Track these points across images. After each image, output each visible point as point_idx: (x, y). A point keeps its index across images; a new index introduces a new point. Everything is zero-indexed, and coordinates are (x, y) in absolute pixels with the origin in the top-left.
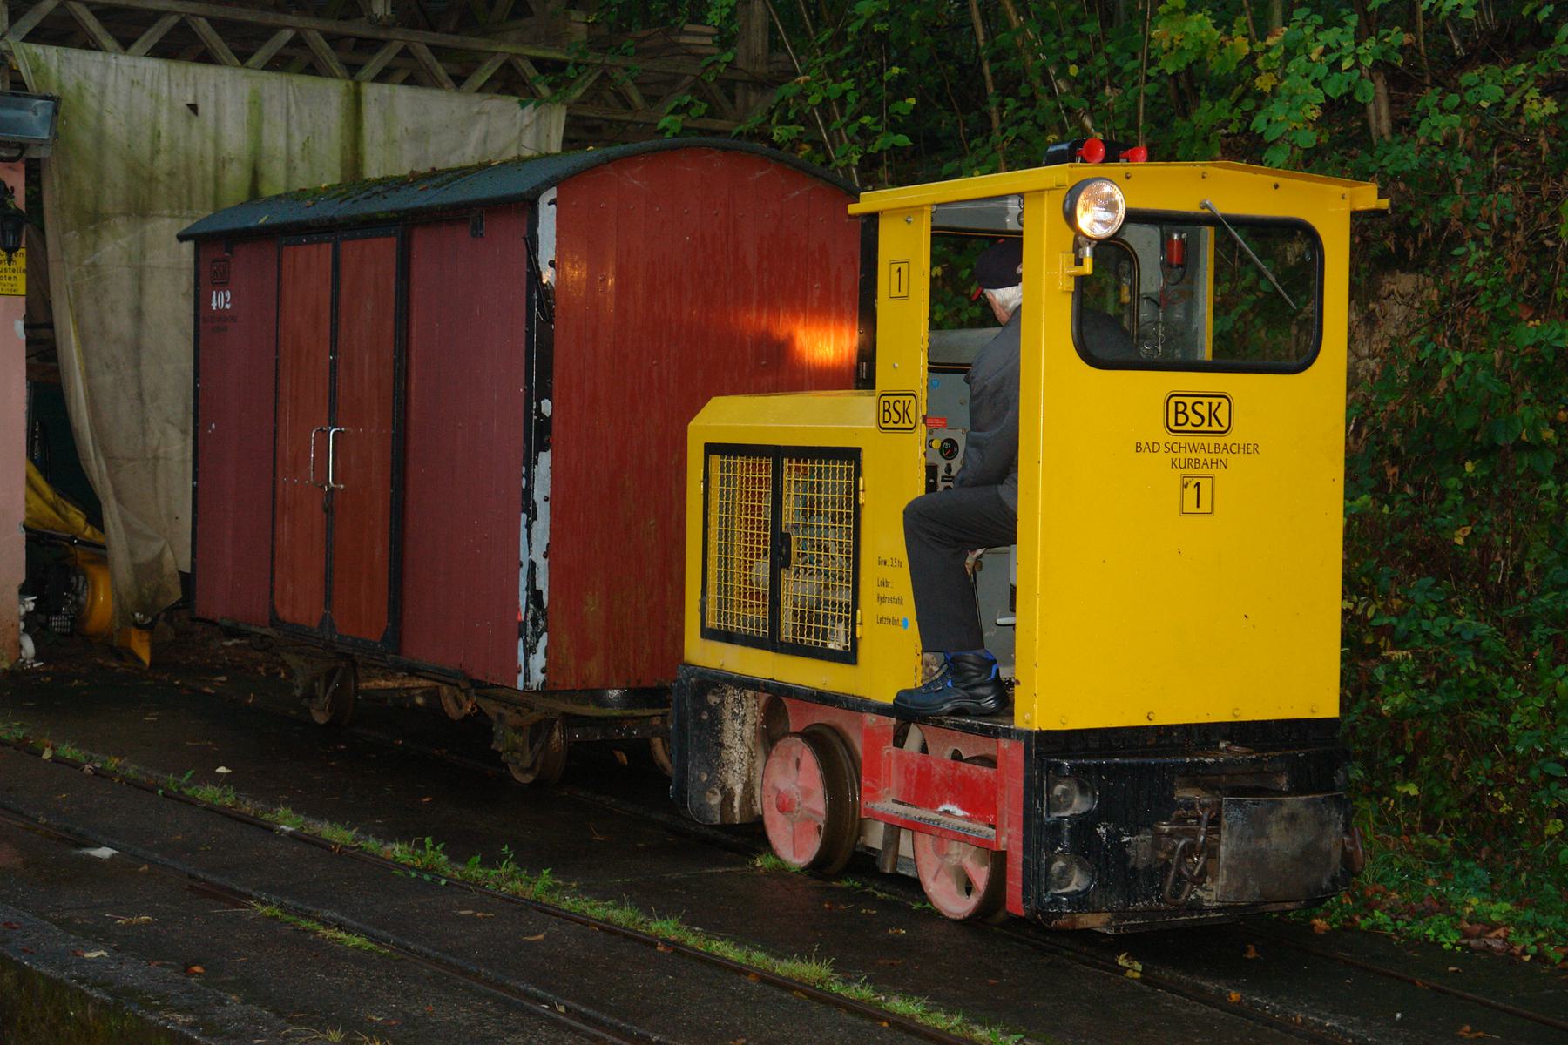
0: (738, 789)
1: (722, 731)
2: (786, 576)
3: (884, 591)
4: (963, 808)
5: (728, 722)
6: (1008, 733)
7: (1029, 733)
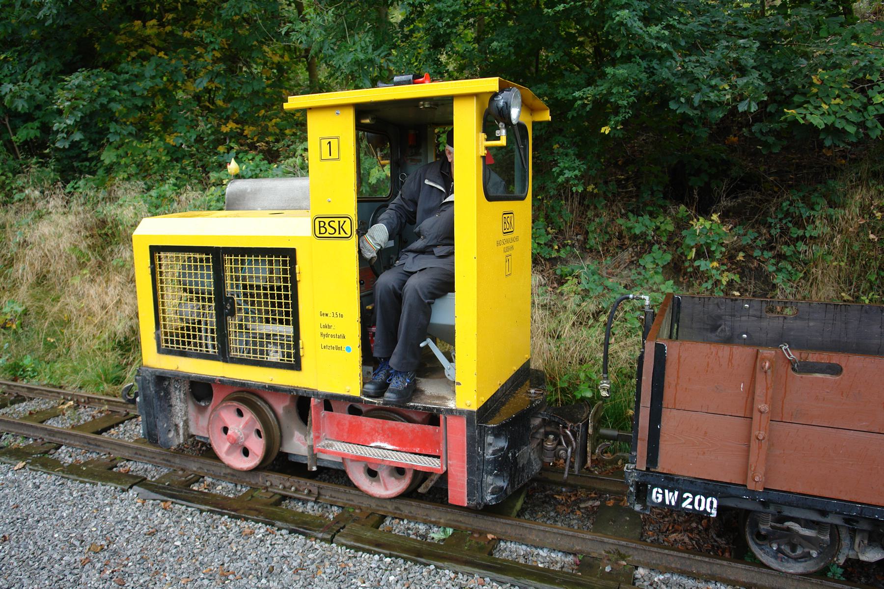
0: (181, 425)
1: (171, 398)
2: (233, 323)
3: (325, 331)
4: (393, 445)
5: (173, 393)
6: (451, 411)
7: (470, 414)
